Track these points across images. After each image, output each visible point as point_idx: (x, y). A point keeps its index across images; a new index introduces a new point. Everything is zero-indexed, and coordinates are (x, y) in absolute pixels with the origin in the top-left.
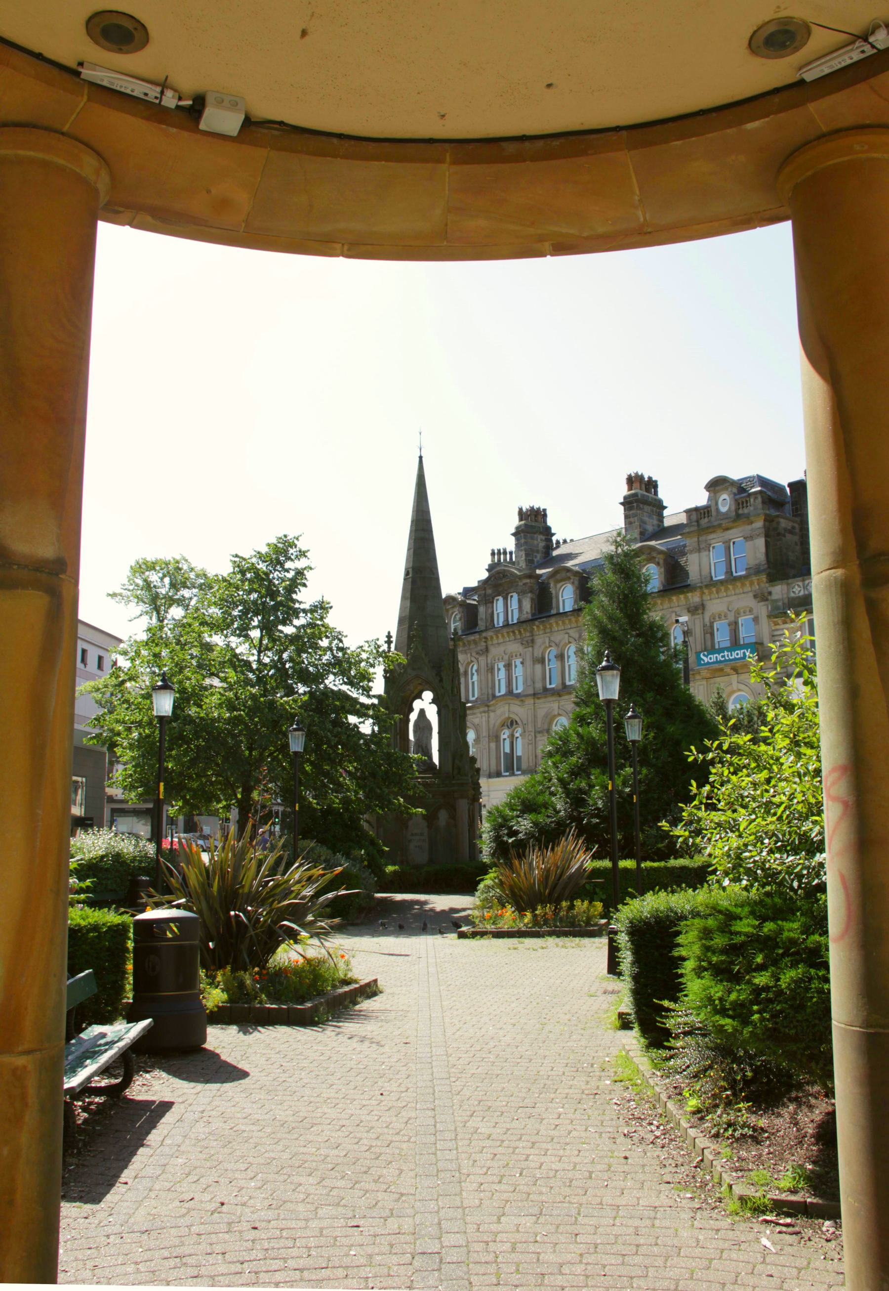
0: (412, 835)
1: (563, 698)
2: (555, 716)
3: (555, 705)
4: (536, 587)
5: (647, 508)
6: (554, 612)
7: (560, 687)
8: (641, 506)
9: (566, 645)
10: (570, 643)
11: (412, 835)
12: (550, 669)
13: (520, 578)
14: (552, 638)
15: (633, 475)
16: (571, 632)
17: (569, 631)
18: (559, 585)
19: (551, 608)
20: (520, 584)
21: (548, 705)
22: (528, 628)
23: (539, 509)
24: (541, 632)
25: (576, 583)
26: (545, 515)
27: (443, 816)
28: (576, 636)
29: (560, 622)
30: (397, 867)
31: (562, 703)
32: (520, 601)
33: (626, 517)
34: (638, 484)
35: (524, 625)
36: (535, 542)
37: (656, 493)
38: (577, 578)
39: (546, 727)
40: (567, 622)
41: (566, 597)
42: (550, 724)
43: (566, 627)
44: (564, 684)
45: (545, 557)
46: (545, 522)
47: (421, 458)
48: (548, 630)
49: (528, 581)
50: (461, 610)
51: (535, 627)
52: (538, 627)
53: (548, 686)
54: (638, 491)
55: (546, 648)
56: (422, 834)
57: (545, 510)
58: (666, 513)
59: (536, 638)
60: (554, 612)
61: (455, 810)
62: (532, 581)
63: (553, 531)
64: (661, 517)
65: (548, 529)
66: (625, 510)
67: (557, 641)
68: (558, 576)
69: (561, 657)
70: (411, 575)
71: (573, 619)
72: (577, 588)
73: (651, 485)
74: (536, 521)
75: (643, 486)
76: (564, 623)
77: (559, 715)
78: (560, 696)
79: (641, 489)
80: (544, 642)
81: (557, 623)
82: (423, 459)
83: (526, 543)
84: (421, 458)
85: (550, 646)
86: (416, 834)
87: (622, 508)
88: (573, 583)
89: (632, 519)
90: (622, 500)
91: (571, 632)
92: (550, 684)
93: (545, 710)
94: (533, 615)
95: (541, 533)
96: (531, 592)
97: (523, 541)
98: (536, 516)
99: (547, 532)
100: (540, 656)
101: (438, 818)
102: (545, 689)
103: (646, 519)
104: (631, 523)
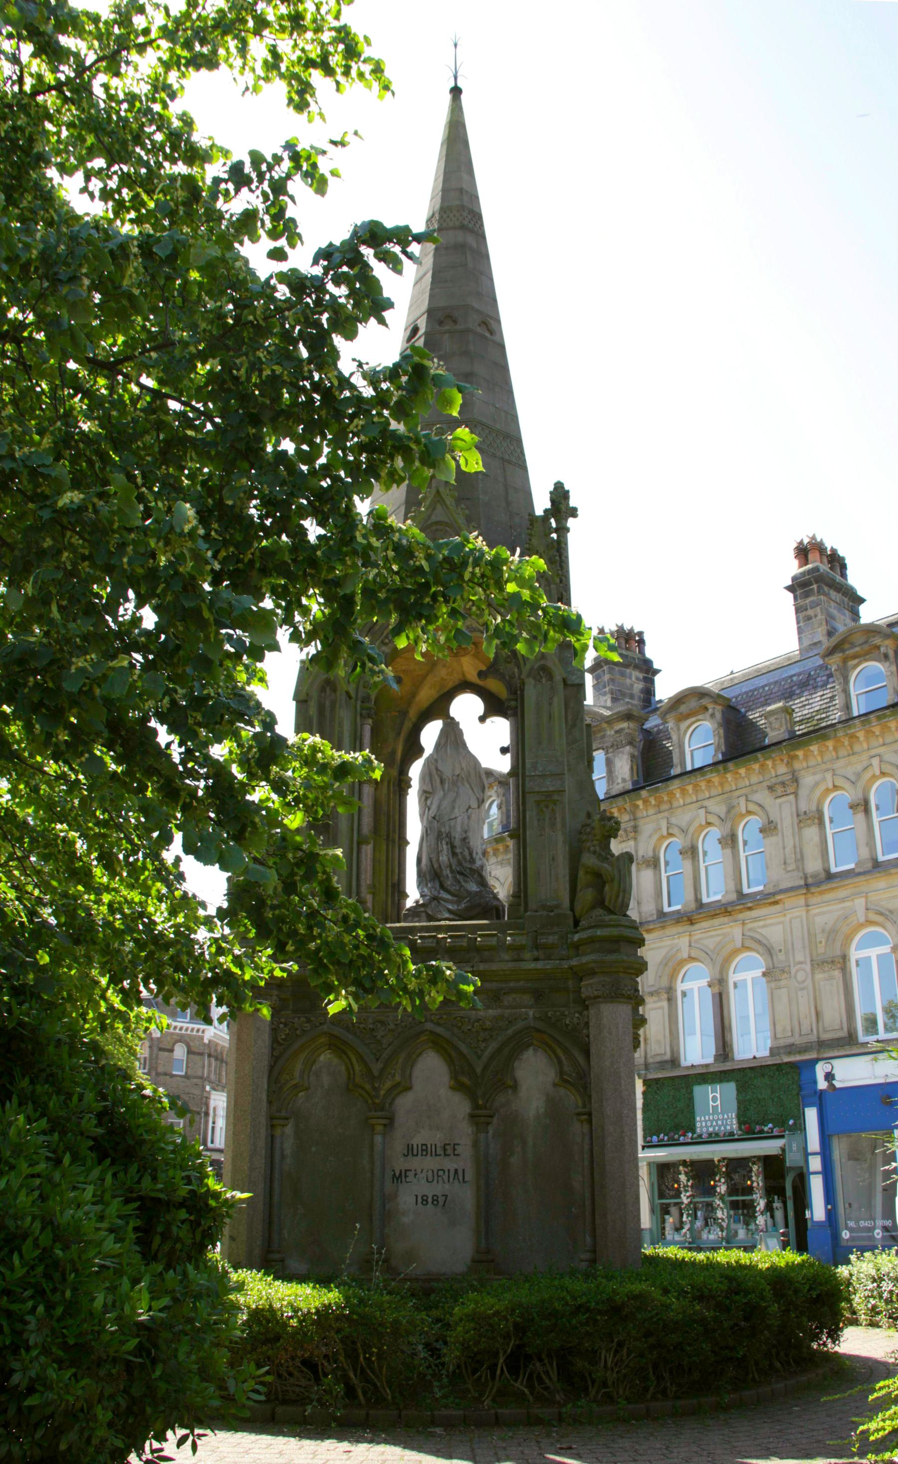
0: (410, 1151)
1: (697, 926)
2: (682, 963)
3: (684, 941)
4: (639, 737)
5: (833, 594)
6: (675, 771)
7: (693, 906)
8: (826, 589)
9: (701, 828)
10: (709, 824)
11: (410, 1151)
12: (668, 877)
13: (609, 721)
14: (673, 820)
15: (806, 541)
16: (712, 805)
17: (705, 803)
18: (684, 725)
19: (672, 766)
20: (610, 732)
21: (668, 942)
22: (627, 806)
23: (631, 630)
24: (651, 811)
25: (718, 715)
26: (641, 642)
27: (535, 1077)
28: (721, 810)
29: (690, 788)
30: (333, 1296)
31: (697, 936)
32: (609, 763)
33: (798, 610)
34: (817, 554)
35: (620, 799)
36: (628, 681)
37: (844, 575)
38: (719, 708)
39: (664, 983)
40: (703, 785)
41: (698, 743)
42: (673, 977)
43: (701, 797)
44: (698, 900)
45: (645, 707)
46: (642, 652)
47: (456, 92)
48: (664, 807)
49: (625, 725)
50: (501, 791)
51: (640, 803)
52: (646, 801)
53: (666, 909)
54: (818, 564)
55: (663, 838)
56: (449, 1149)
57: (640, 634)
58: (862, 609)
59: (641, 823)
60: (675, 771)
61: (587, 1054)
62: (632, 725)
63: (656, 666)
64: (856, 616)
65: (648, 663)
66: (795, 599)
67: (683, 824)
68: (683, 709)
69: (691, 852)
70: (422, 331)
71: (716, 780)
72: (720, 725)
73: (836, 561)
74: (627, 649)
75: (825, 560)
76: (696, 787)
77: (692, 959)
78: (692, 923)
79: (821, 562)
80: (660, 829)
81: (683, 791)
82: (463, 97)
83: (612, 680)
84: (456, 92)
85: (671, 835)
86: (425, 1150)
87: (790, 596)
88: (713, 716)
89: (810, 612)
90: (789, 583)
91: (712, 805)
92: (669, 905)
93: (664, 952)
94: (635, 783)
95: (636, 667)
96: (630, 743)
97: (607, 677)
98: (627, 641)
99: (648, 671)
100: (651, 854)
101: (515, 1087)
102: (661, 914)
103: (835, 612)
104: (809, 618)
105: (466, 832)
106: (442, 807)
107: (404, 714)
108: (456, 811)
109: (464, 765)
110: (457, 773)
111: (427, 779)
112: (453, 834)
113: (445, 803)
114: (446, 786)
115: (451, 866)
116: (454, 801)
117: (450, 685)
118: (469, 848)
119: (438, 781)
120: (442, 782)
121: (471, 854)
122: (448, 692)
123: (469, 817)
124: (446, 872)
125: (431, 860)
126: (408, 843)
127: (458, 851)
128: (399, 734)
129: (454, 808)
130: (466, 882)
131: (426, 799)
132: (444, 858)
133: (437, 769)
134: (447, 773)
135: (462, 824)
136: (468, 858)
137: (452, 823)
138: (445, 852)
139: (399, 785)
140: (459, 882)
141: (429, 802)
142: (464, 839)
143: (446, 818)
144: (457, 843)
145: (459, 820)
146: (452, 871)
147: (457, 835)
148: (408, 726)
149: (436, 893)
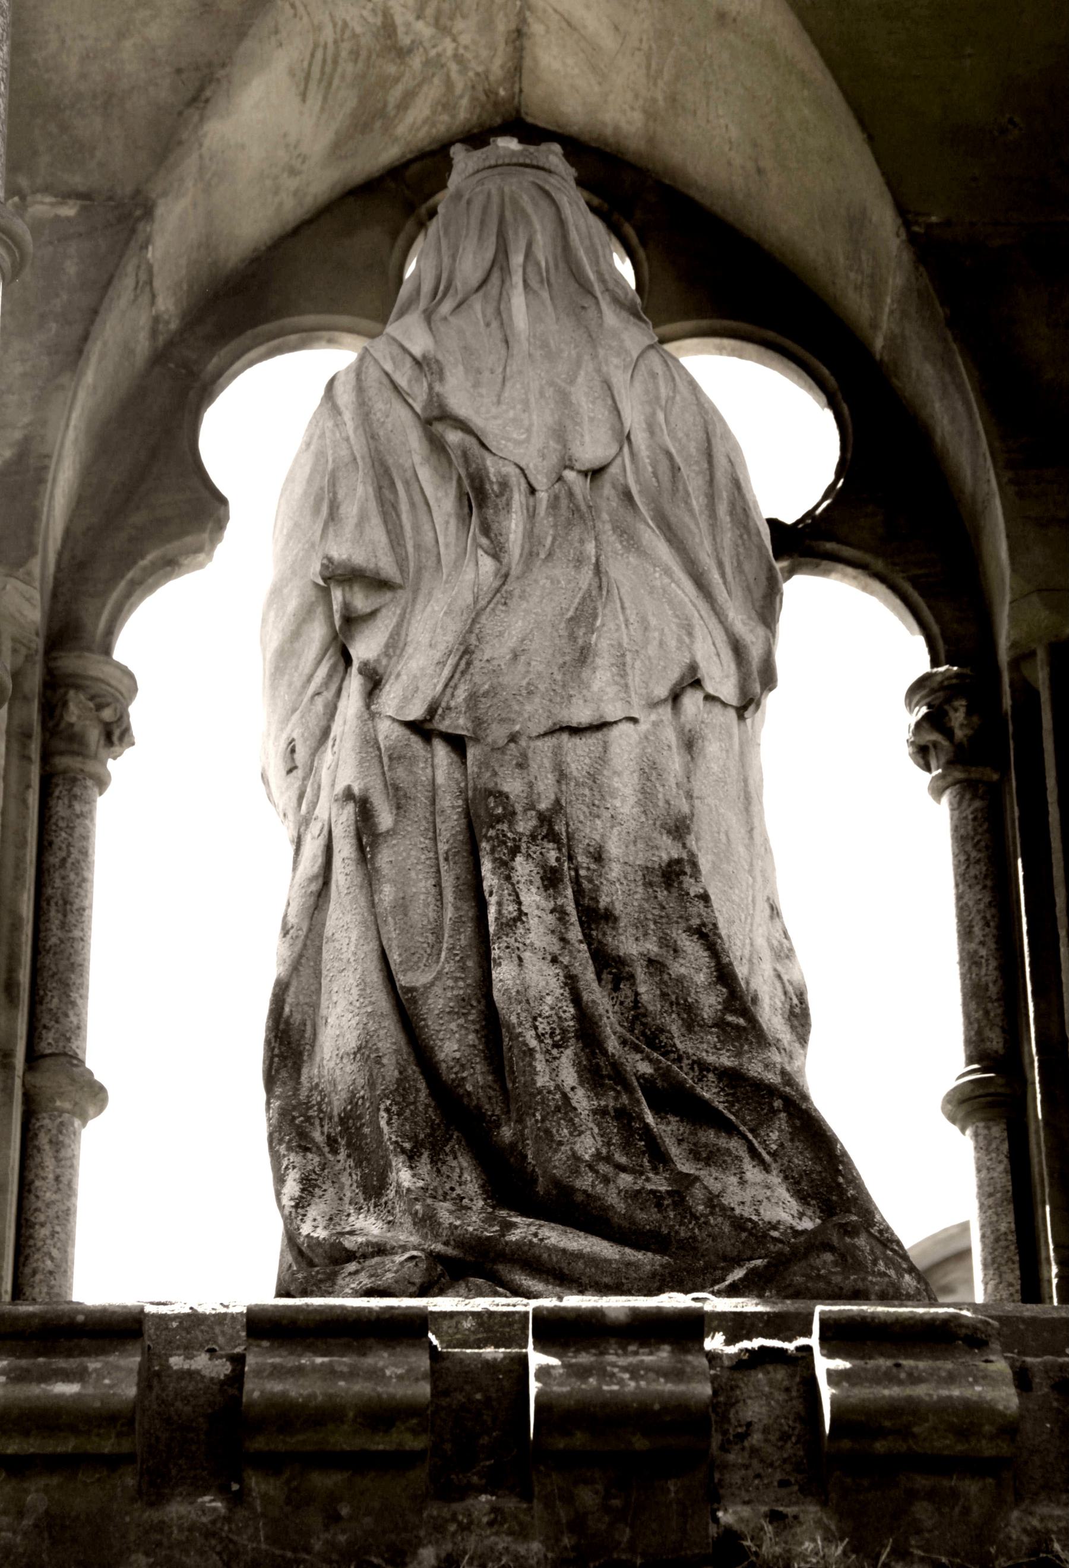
105: (679, 828)
106: (495, 650)
107: (122, 217)
108: (601, 677)
109: (633, 418)
110: (592, 449)
111: (358, 495)
112: (589, 831)
113: (526, 628)
114: (514, 527)
115: (587, 1030)
116: (583, 617)
117: (416, 124)
118: (708, 937)
119: (444, 503)
120: (477, 497)
121: (724, 975)
122: (395, 172)
123: (690, 744)
124: (560, 1072)
125: (405, 1008)
126: (95, 1095)
127: (630, 945)
128: (74, 355)
129: (584, 656)
130: (709, 1157)
131: (352, 621)
132: (530, 975)
133: (436, 419)
134: (518, 436)
135: (650, 772)
136: (710, 1003)
137: (578, 753)
138: (538, 931)
139: (52, 707)
140: (659, 1157)
141: (365, 648)
142: (674, 875)
143: (534, 715)
144: (618, 891)
145: (624, 742)
146: (599, 1072)
147: (619, 838)
148: (127, 330)
149: (475, 1221)
